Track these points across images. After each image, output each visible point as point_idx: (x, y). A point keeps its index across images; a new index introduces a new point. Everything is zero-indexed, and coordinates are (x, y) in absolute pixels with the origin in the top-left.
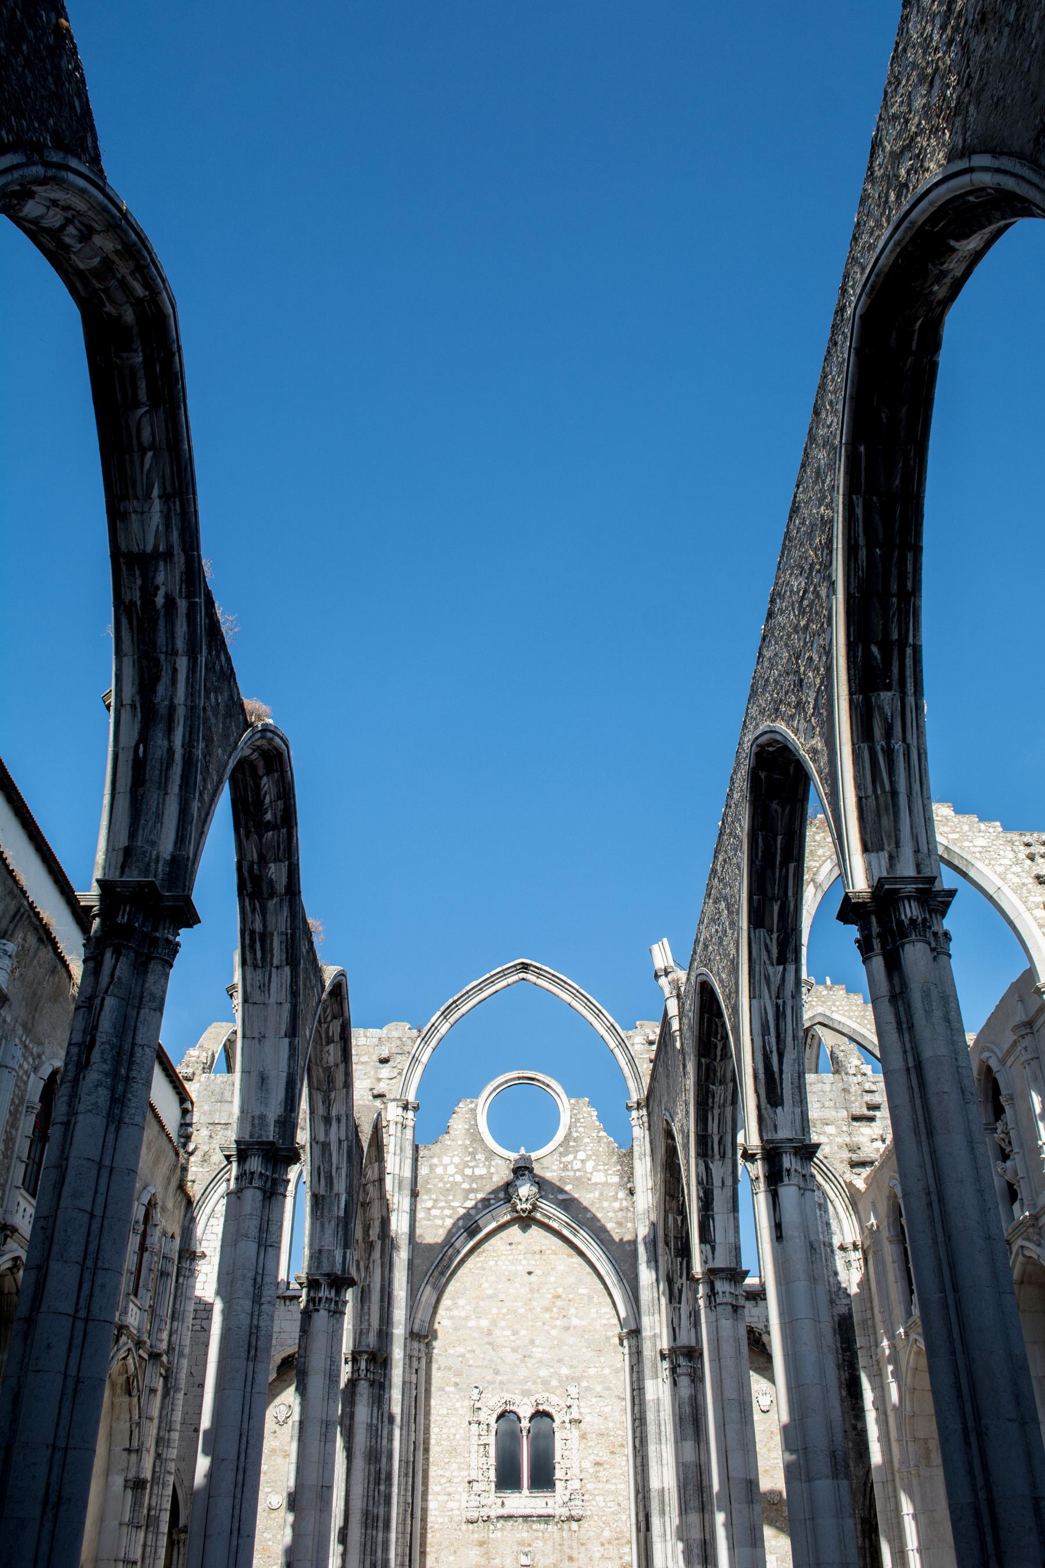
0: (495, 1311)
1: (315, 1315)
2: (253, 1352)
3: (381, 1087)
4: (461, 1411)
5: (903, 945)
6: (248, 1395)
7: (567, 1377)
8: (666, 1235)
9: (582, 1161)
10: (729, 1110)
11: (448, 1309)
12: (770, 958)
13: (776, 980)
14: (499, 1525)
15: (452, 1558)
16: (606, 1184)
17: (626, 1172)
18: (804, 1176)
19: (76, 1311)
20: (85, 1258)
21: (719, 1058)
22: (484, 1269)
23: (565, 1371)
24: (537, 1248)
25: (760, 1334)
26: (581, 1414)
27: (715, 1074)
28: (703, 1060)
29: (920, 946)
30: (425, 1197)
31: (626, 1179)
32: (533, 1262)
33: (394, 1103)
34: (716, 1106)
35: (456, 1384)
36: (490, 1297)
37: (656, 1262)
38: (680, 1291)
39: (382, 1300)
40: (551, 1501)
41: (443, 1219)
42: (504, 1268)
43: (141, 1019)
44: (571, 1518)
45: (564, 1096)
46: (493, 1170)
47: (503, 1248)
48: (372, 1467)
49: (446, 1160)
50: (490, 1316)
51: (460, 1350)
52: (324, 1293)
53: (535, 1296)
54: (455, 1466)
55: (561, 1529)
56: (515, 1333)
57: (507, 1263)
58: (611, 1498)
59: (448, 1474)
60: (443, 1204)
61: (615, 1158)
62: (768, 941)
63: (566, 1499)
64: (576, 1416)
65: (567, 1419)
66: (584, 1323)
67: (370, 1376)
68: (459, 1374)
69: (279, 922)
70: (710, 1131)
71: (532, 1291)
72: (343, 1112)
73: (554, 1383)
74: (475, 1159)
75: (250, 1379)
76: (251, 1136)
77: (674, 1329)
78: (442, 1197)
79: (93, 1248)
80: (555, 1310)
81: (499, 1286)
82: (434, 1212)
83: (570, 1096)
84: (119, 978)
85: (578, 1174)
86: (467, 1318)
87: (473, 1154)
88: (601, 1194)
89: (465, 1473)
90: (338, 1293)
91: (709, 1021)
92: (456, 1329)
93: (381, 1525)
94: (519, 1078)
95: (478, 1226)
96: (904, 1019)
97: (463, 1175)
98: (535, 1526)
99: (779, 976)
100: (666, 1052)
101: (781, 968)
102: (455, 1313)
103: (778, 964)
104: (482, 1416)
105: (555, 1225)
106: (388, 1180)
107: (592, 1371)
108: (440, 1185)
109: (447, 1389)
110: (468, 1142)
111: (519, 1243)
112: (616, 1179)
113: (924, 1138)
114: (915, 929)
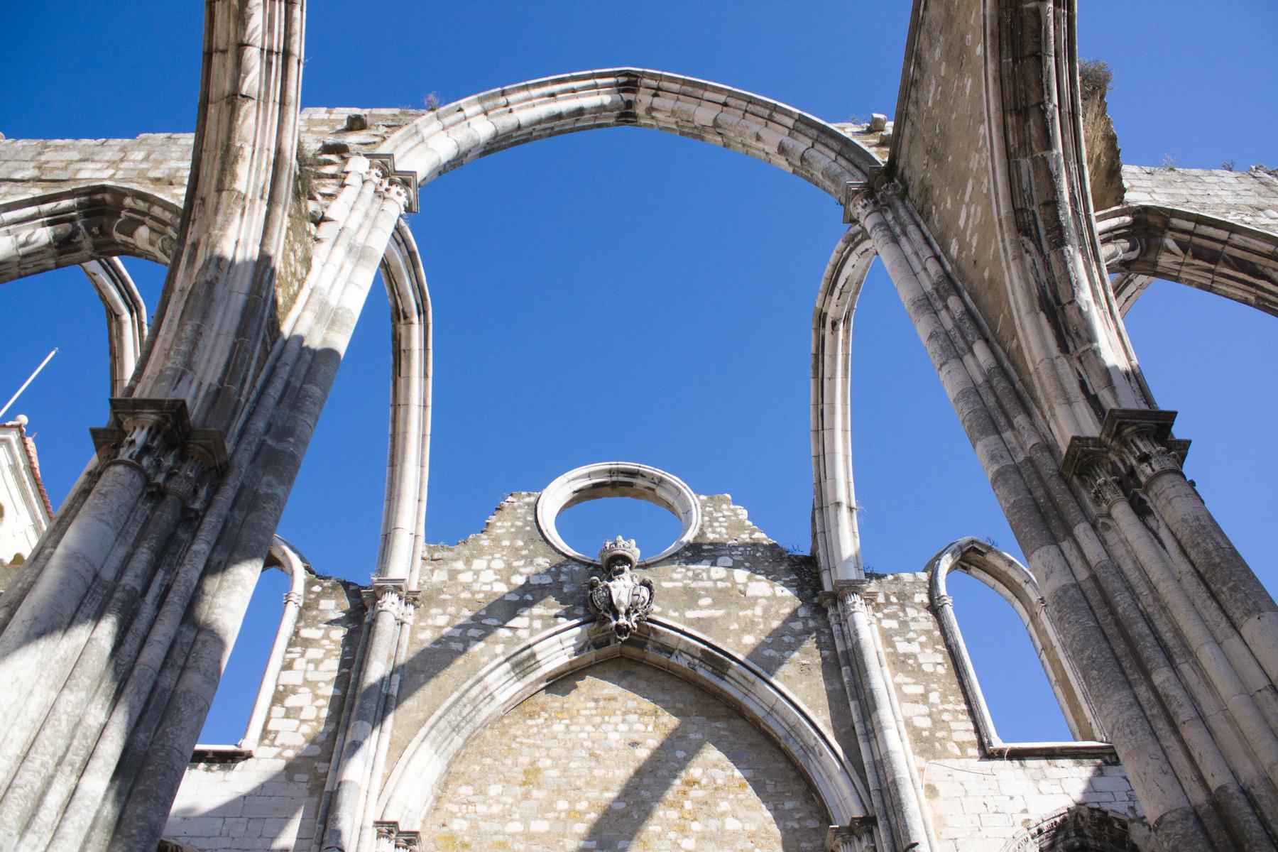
25: (1124, 825)
30: (434, 611)
31: (809, 592)
32: (641, 727)
42: (583, 735)
45: (687, 491)
46: (563, 578)
49: (478, 564)
50: (551, 815)
53: (646, 781)
57: (589, 728)
80: (688, 805)
81: (572, 765)
83: (698, 491)
85: (720, 584)
86: (505, 817)
94: (611, 472)
95: (533, 655)
105: (682, 662)
110: (520, 543)
111: (611, 699)
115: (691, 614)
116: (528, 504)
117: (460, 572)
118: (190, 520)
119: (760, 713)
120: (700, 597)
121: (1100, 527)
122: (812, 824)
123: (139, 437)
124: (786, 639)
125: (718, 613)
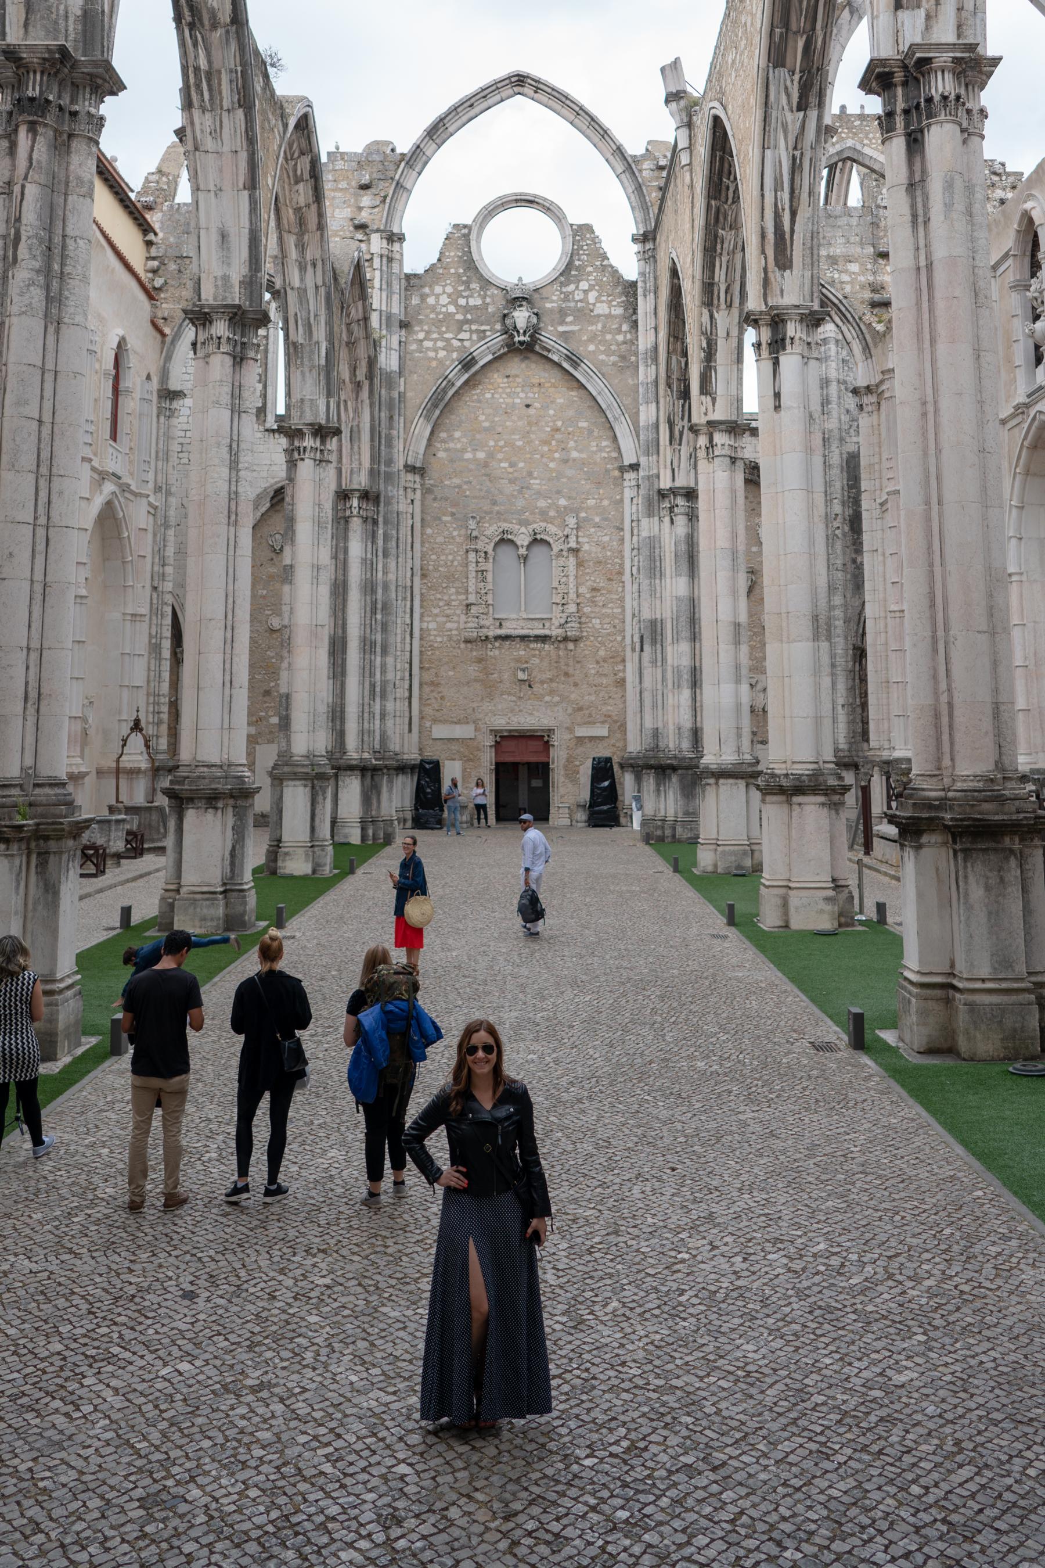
0: (492, 443)
1: (300, 463)
2: (233, 517)
3: (364, 217)
4: (458, 540)
5: (929, 125)
6: (231, 559)
7: (565, 507)
8: (668, 377)
9: (585, 292)
10: (739, 256)
11: (444, 441)
12: (789, 102)
13: (794, 129)
14: (497, 644)
15: (451, 673)
16: (609, 316)
17: (631, 303)
18: (809, 344)
19: (36, 518)
20: (38, 466)
21: (730, 201)
22: (480, 401)
23: (563, 502)
24: (535, 381)
26: (578, 542)
27: (725, 218)
28: (713, 203)
29: (949, 127)
33: (378, 235)
34: (725, 253)
35: (453, 514)
36: (486, 429)
37: (658, 403)
38: (681, 434)
39: (372, 440)
40: (547, 625)
41: (436, 350)
43: (69, 207)
44: (566, 639)
46: (488, 300)
47: (500, 380)
48: (368, 598)
49: (438, 289)
51: (456, 481)
52: (309, 442)
54: (453, 590)
55: (558, 648)
56: (511, 465)
58: (607, 620)
59: (446, 598)
60: (435, 336)
61: (619, 289)
62: (789, 83)
63: (563, 621)
64: (573, 545)
65: (565, 547)
66: (584, 456)
67: (363, 513)
68: (455, 505)
69: (227, 58)
70: (716, 279)
71: (530, 424)
72: (318, 256)
73: (552, 513)
74: (468, 288)
75: (232, 542)
76: (215, 299)
77: (673, 470)
78: (434, 329)
79: (45, 455)
80: (554, 443)
82: (428, 344)
84: (39, 162)
85: (579, 305)
86: (463, 450)
87: (467, 284)
88: (604, 327)
89: (463, 597)
90: (323, 442)
91: (722, 159)
92: (452, 461)
93: (378, 649)
96: (920, 212)
97: (457, 305)
98: (532, 646)
99: (798, 124)
100: (676, 185)
101: (802, 113)
102: (451, 445)
103: (799, 109)
104: (480, 545)
105: (555, 358)
106: (375, 318)
107: (591, 502)
108: (432, 316)
109: (445, 518)
112: (620, 311)
113: (927, 344)
114: (945, 107)
115: (561, 329)
116: (464, 235)
117: (428, 295)
118: (375, 522)
119: (594, 393)
120: (566, 315)
121: (660, 520)
122: (615, 455)
123: (355, 503)
124: (613, 347)
125: (576, 328)
